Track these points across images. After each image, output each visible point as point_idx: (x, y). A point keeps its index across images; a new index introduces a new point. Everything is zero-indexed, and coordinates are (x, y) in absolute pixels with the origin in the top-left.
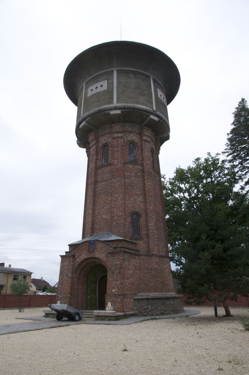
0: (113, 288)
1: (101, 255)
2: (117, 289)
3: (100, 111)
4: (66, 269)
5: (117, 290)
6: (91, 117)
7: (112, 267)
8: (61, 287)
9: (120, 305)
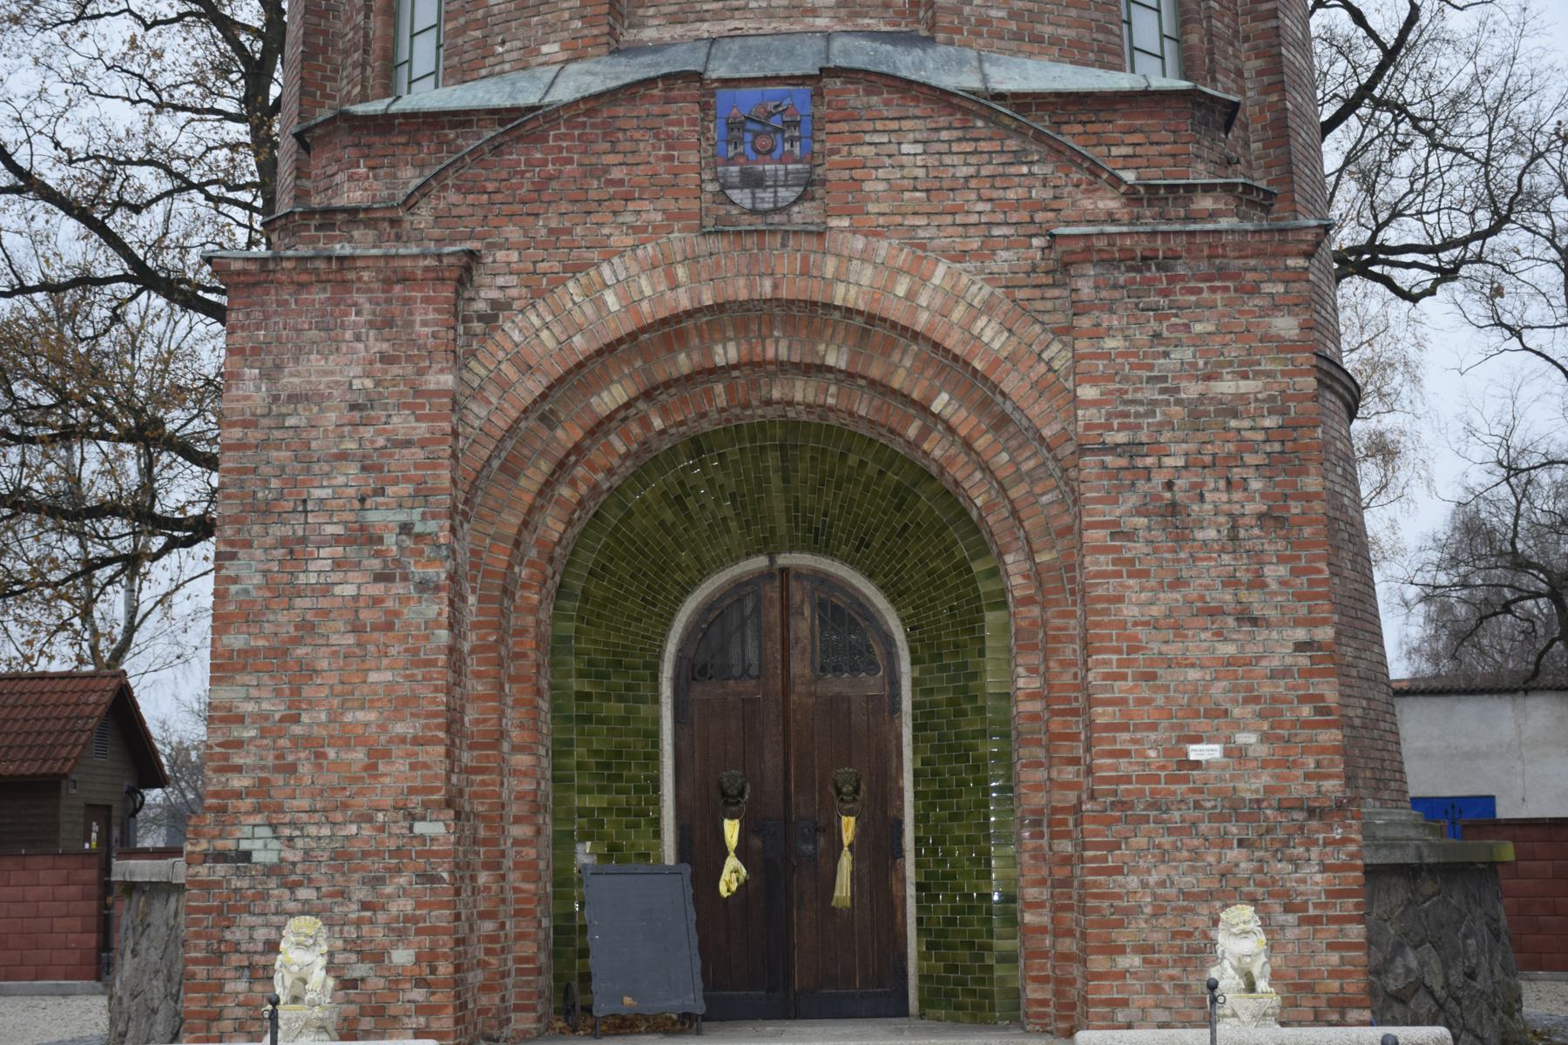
0: (1200, 725)
1: (924, 280)
2: (1265, 738)
4: (343, 456)
5: (1262, 751)
7: (1143, 436)
8: (277, 708)
9: (1332, 947)
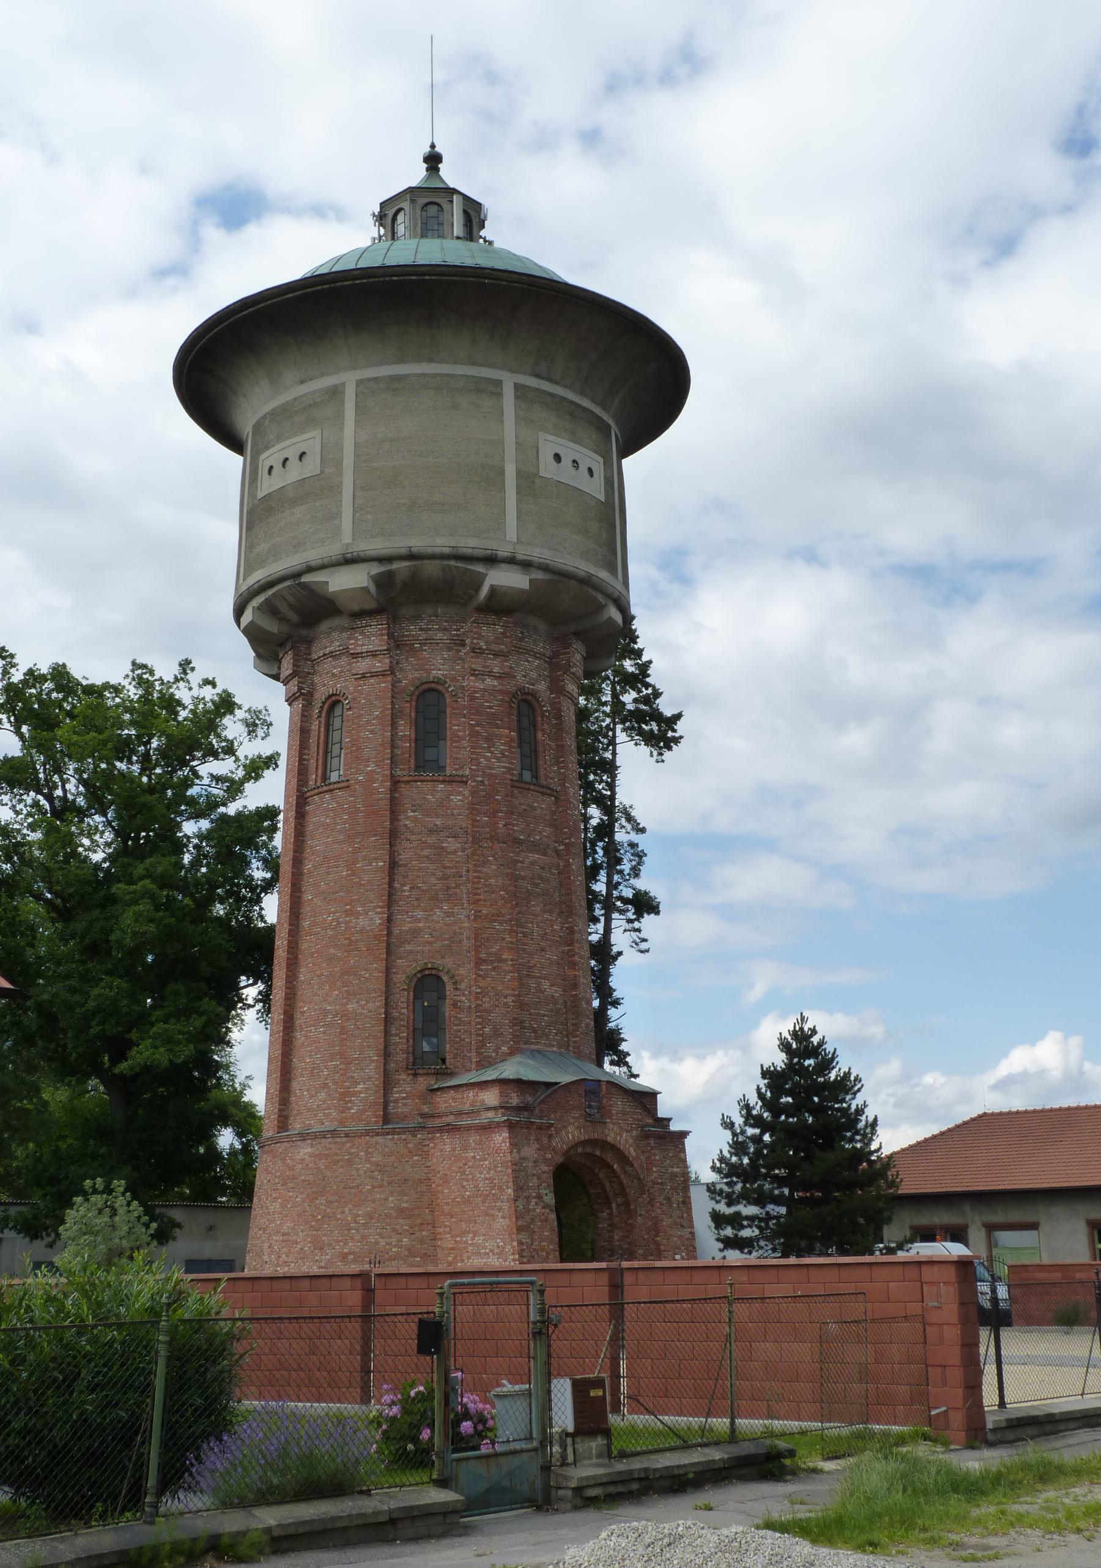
3: (587, 581)
4: (534, 1175)
6: (556, 577)
